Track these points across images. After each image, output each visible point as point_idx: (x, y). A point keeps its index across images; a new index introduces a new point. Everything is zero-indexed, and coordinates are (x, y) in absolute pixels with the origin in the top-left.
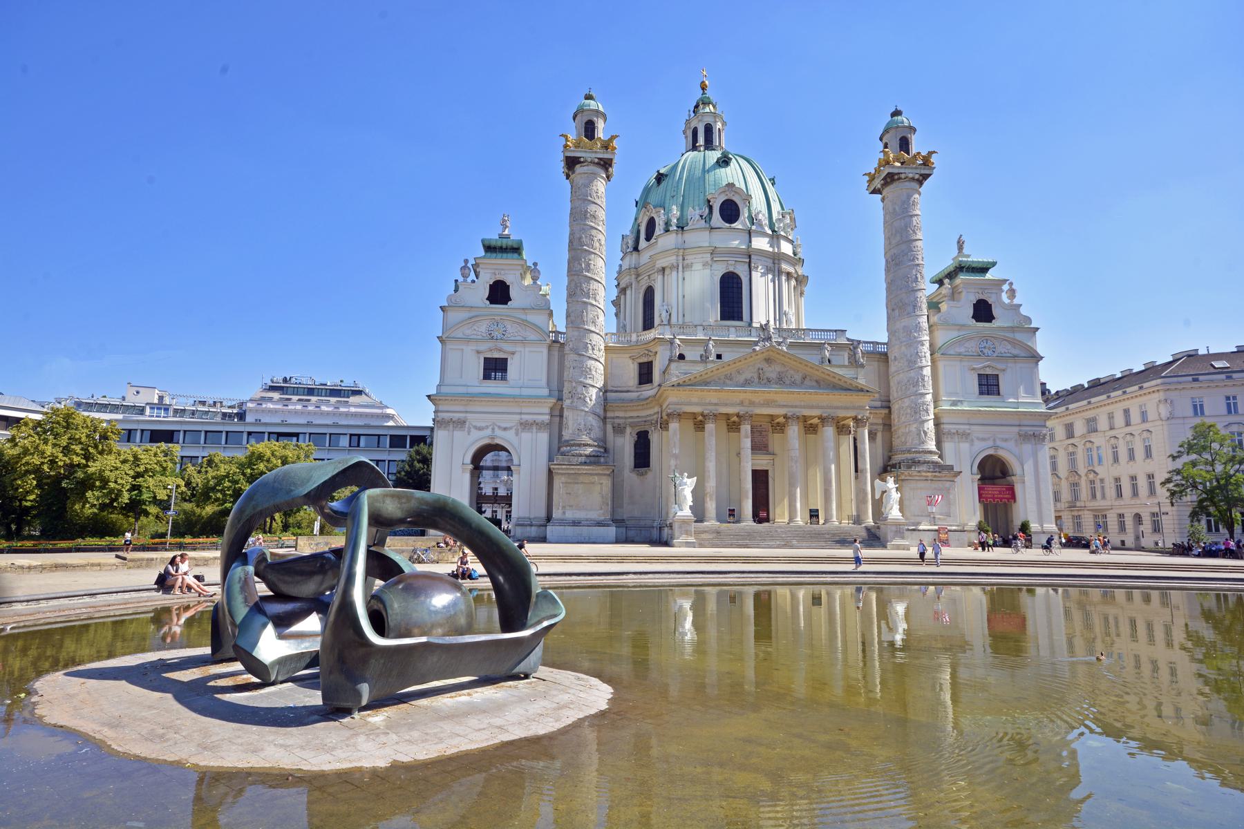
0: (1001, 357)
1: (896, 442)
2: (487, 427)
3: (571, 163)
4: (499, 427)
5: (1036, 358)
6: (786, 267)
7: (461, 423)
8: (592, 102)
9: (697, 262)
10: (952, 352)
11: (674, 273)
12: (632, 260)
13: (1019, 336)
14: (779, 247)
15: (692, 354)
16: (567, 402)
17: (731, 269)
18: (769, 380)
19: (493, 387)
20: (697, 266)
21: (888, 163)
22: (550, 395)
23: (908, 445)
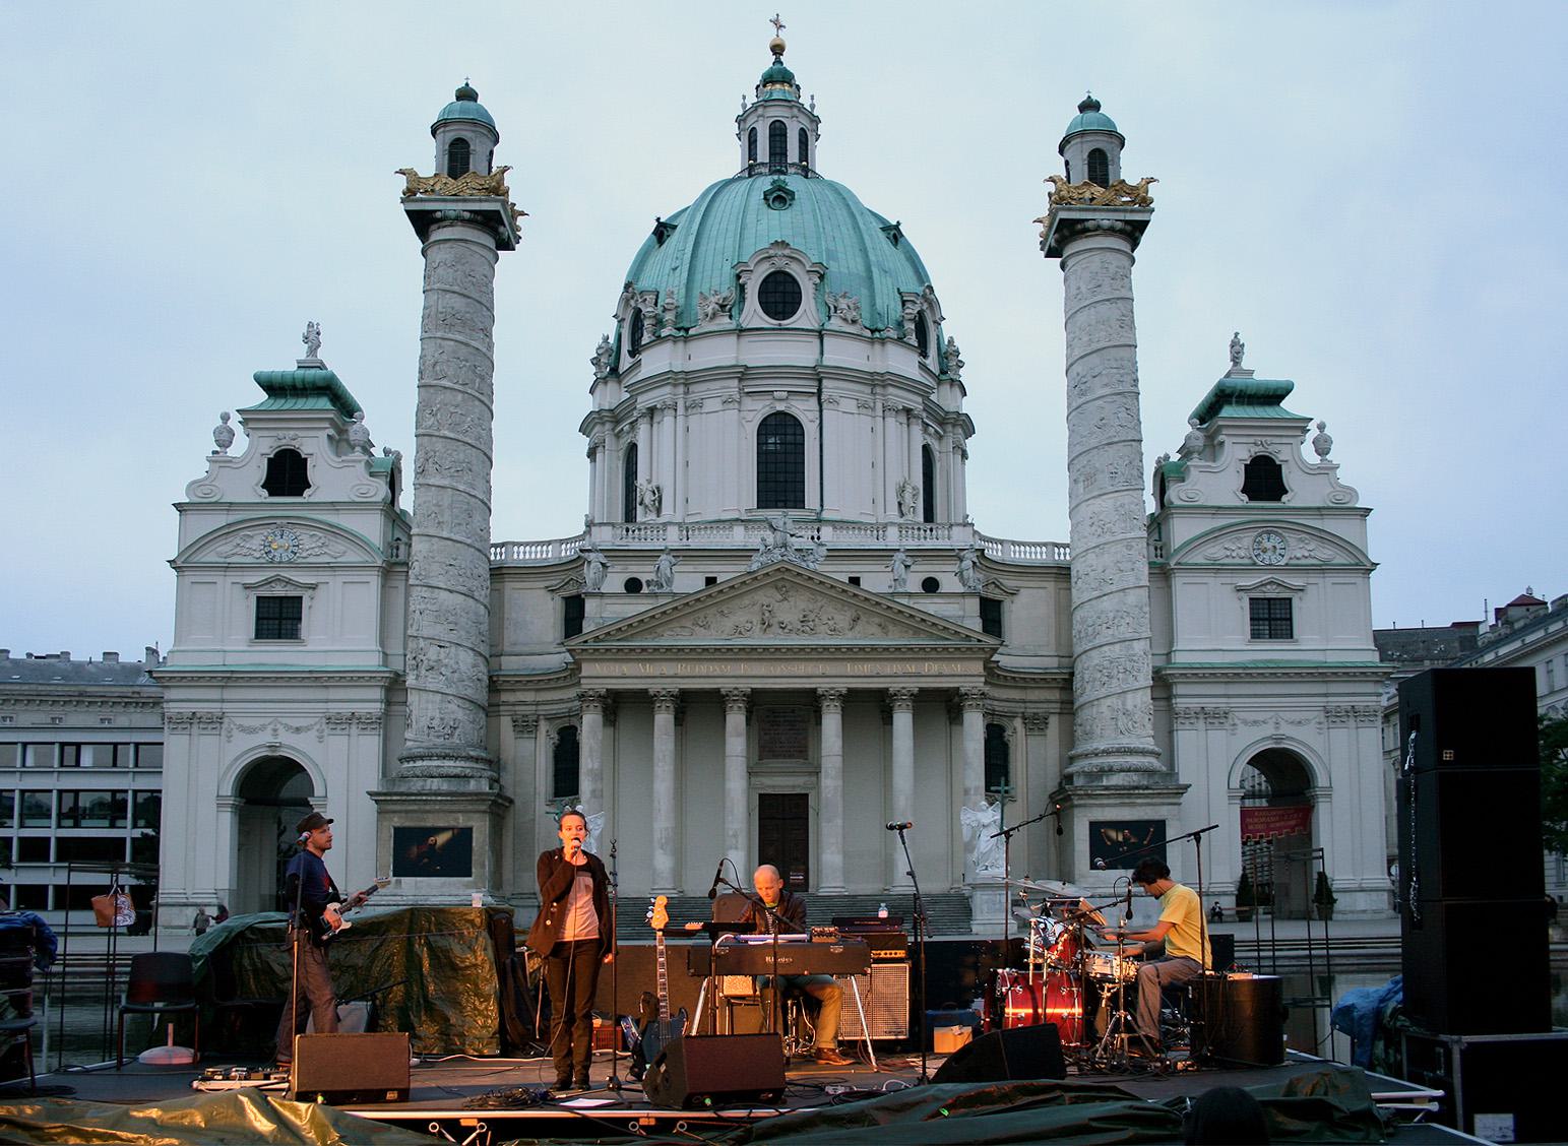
0: (1293, 568)
4: (288, 728)
5: (1367, 568)
6: (899, 398)
9: (712, 394)
10: (1197, 558)
13: (1331, 525)
16: (410, 681)
17: (780, 407)
19: (277, 655)
20: (712, 405)
22: (385, 664)
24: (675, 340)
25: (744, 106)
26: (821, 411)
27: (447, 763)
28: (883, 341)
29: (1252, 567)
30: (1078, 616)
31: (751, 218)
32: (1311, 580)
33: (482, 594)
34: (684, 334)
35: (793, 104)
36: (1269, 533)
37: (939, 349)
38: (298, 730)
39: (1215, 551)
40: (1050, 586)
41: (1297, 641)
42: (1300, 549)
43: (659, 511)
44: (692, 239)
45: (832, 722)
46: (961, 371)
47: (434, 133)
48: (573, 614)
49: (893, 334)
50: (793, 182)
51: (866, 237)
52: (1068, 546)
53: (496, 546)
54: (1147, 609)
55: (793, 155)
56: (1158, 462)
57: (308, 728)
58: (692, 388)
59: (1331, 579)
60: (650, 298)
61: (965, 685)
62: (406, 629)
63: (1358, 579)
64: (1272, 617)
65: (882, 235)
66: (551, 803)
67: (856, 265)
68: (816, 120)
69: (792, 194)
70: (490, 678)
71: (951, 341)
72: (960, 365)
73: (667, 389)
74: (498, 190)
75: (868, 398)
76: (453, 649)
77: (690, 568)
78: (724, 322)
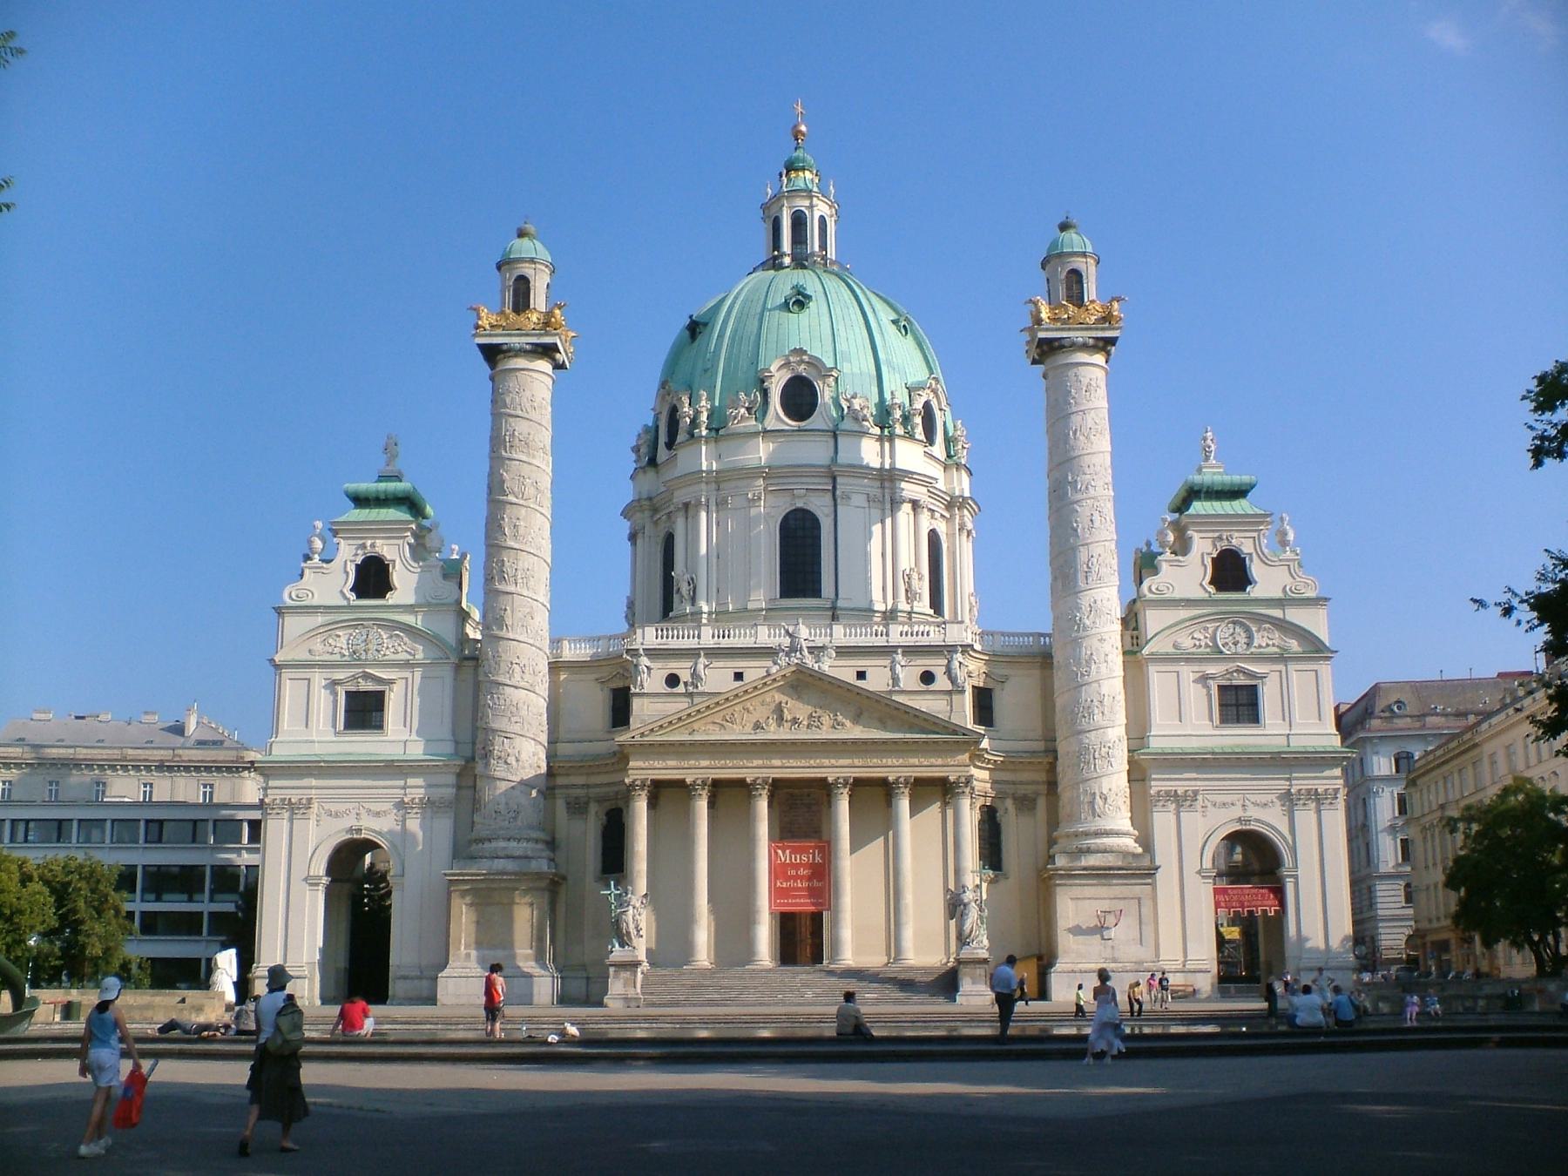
1: (1063, 812)
2: (347, 813)
3: (492, 354)
8: (525, 240)
11: (703, 515)
12: (649, 481)
13: (1295, 616)
14: (892, 456)
15: (685, 676)
16: (479, 768)
17: (800, 505)
18: (795, 721)
19: (363, 745)
21: (1039, 321)
22: (456, 753)
27: (513, 844)
29: (1217, 654)
30: (1060, 702)
36: (1234, 623)
40: (1037, 673)
42: (1265, 640)
45: (843, 806)
48: (620, 710)
49: (899, 430)
52: (1049, 635)
54: (1121, 697)
59: (1292, 667)
60: (686, 400)
62: (475, 719)
66: (598, 880)
69: (809, 298)
73: (703, 486)
75: (878, 492)
76: (518, 740)
77: (721, 664)
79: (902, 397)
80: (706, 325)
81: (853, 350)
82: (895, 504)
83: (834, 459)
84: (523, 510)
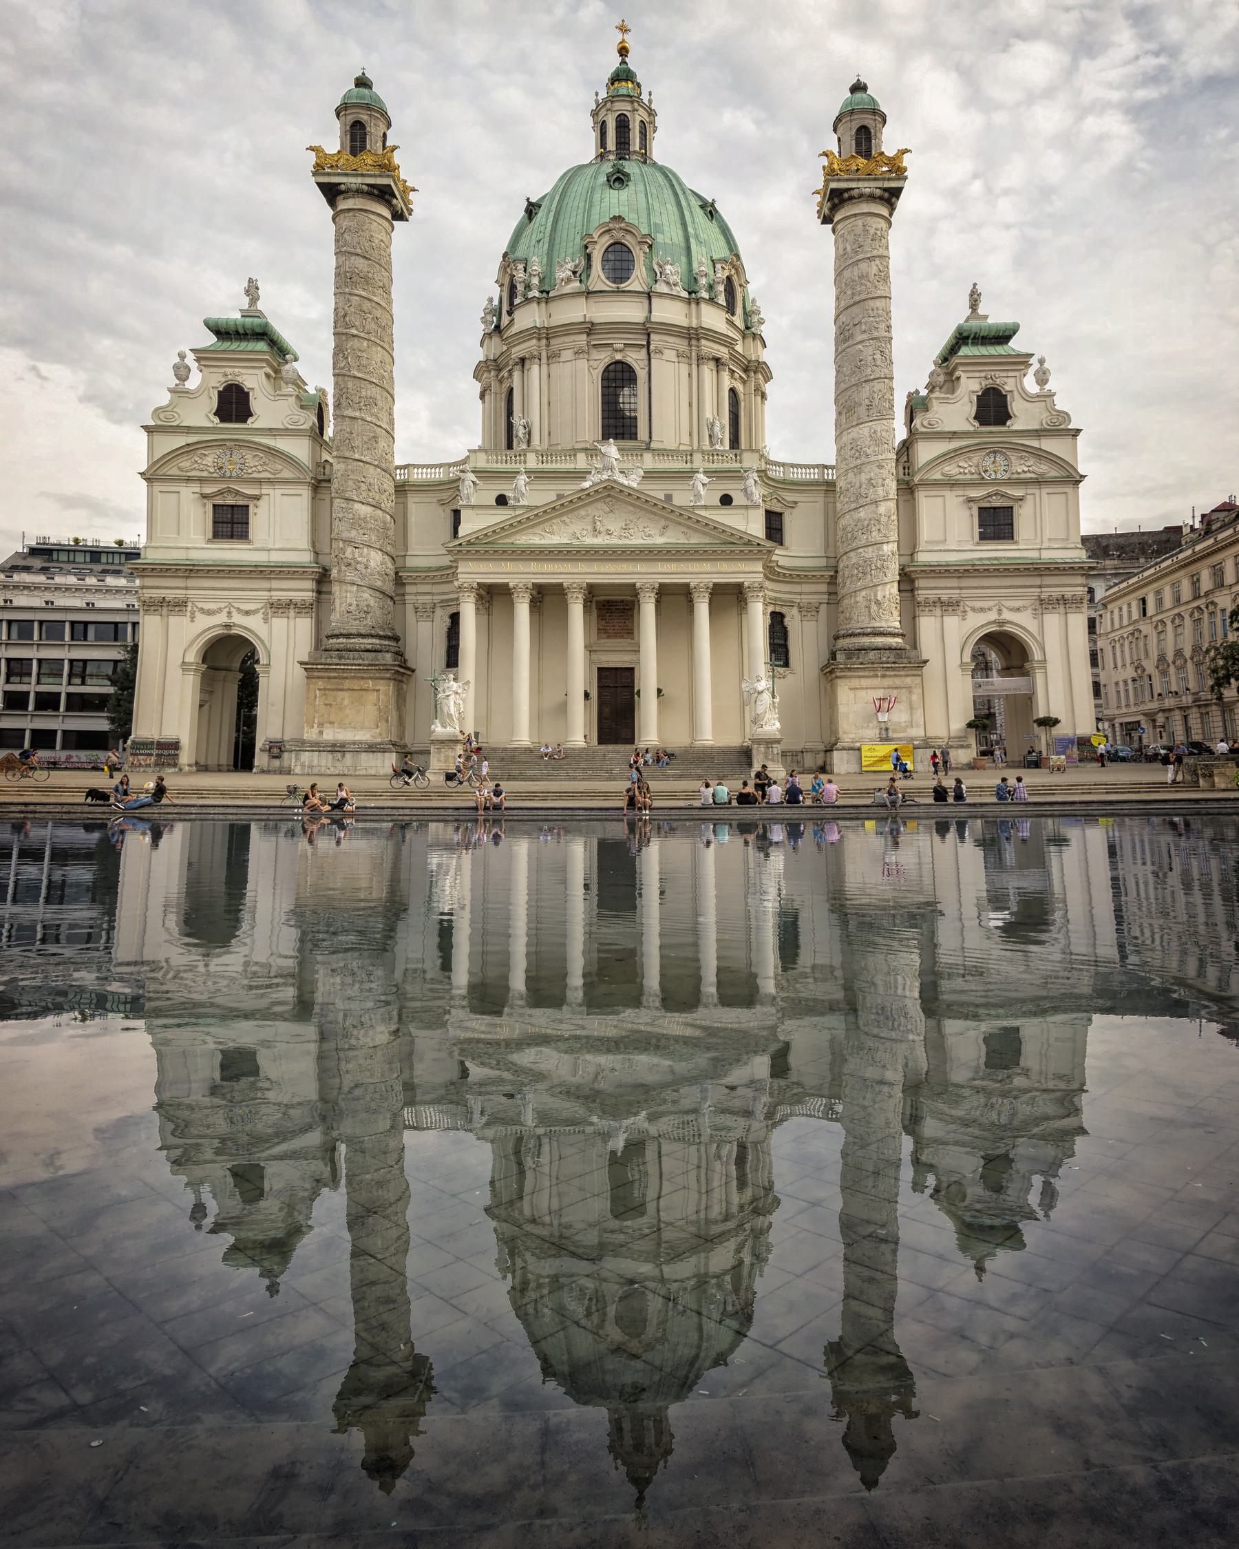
5: (1076, 480)
6: (709, 347)
7: (179, 606)
10: (938, 476)
14: (699, 316)
17: (619, 357)
20: (567, 355)
23: (854, 626)
24: (539, 301)
25: (597, 101)
26: (649, 360)
27: (361, 641)
28: (698, 301)
29: (981, 482)
30: (843, 522)
31: (597, 196)
32: (1029, 491)
33: (389, 505)
34: (546, 297)
35: (633, 99)
37: (744, 308)
38: (247, 613)
39: (951, 469)
40: (820, 499)
41: (1017, 543)
42: (1022, 467)
43: (529, 442)
44: (552, 214)
46: (762, 327)
47: (338, 116)
49: (705, 295)
50: (630, 167)
51: (687, 213)
52: (832, 467)
53: (400, 467)
55: (635, 145)
56: (910, 395)
57: (255, 612)
58: (553, 342)
60: (521, 266)
61: (747, 580)
63: (1069, 489)
64: (996, 523)
65: (700, 212)
67: (678, 237)
68: (651, 113)
69: (627, 175)
70: (397, 573)
71: (754, 301)
72: (761, 322)
73: (534, 342)
74: (388, 168)
78: (575, 285)
79: (707, 268)
80: (540, 206)
81: (666, 223)
82: (700, 359)
83: (648, 320)
84: (365, 344)
